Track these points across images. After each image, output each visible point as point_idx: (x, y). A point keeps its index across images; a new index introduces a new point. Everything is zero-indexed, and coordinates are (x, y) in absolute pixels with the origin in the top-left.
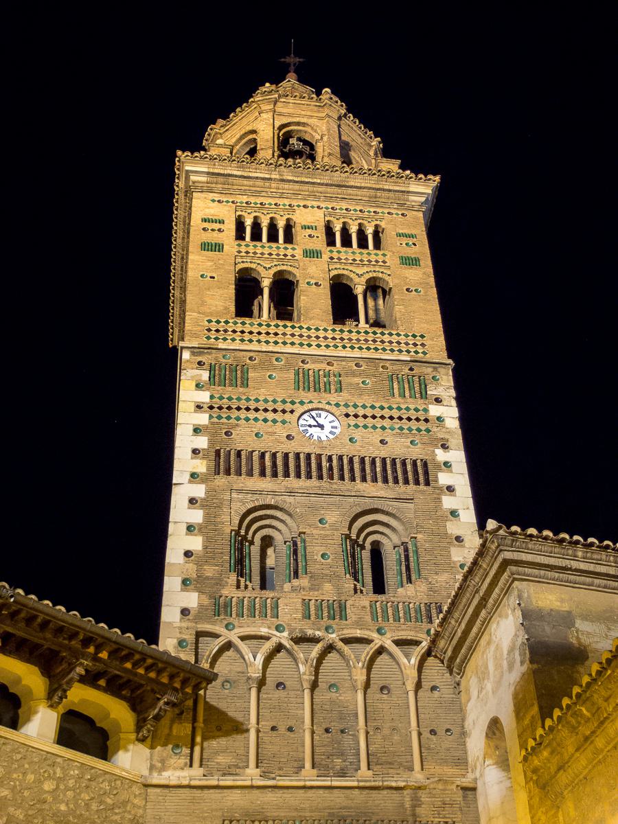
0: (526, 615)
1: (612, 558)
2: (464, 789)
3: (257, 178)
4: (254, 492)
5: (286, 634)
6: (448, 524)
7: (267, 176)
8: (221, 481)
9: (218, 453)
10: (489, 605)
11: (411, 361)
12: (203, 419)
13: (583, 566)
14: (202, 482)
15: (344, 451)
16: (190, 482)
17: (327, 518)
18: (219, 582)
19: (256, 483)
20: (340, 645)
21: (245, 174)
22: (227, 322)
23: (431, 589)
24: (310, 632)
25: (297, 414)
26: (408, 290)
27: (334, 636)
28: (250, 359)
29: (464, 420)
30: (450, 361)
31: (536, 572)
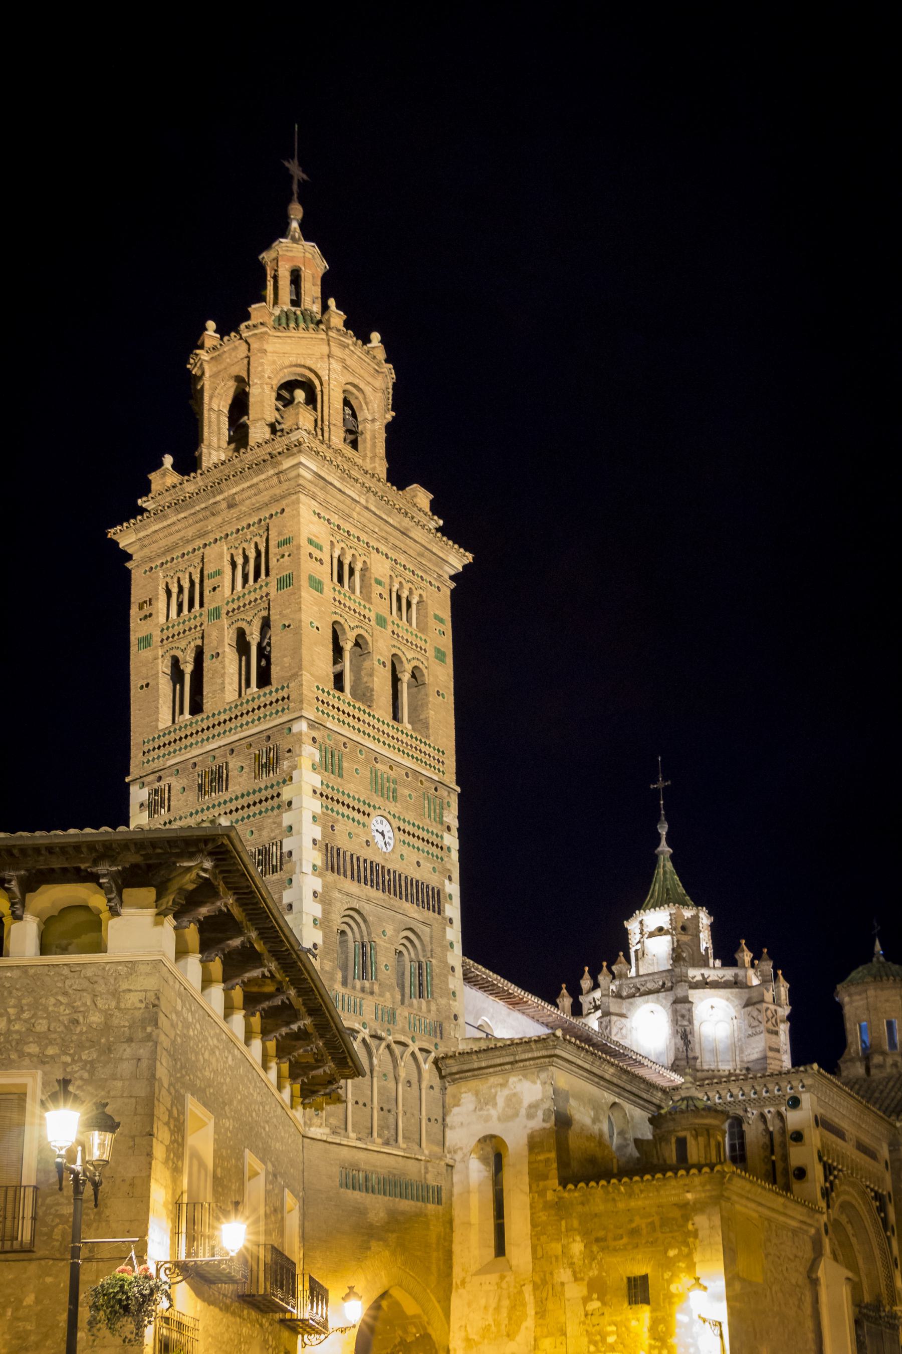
0: (555, 1091)
2: (448, 1165)
4: (347, 894)
5: (367, 1031)
6: (449, 954)
8: (331, 877)
9: (327, 845)
10: (517, 1065)
14: (321, 875)
16: (313, 874)
17: (387, 931)
20: (394, 1046)
23: (438, 1010)
26: (438, 692)
27: (390, 1038)
29: (460, 851)
30: (459, 789)
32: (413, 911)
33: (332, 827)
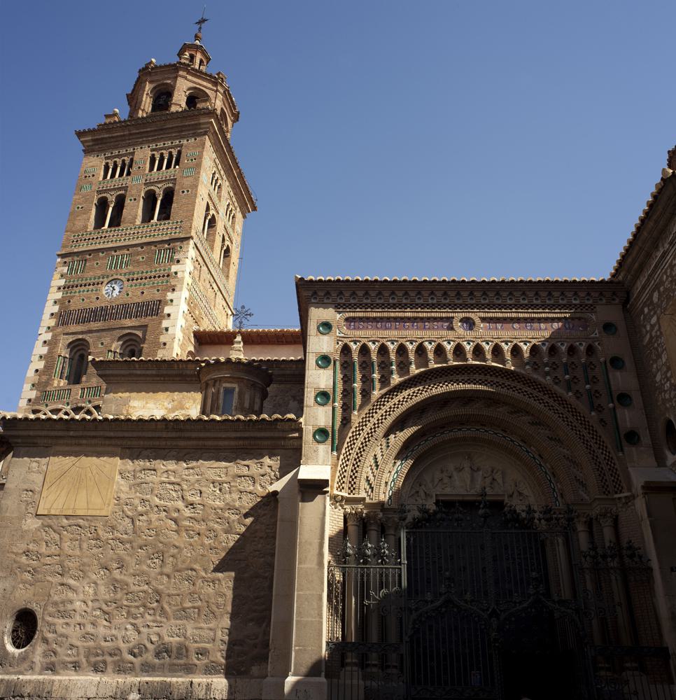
1: (154, 366)
3: (117, 136)
7: (122, 134)
8: (59, 330)
11: (169, 240)
12: (59, 295)
13: (139, 372)
14: (52, 331)
15: (121, 302)
17: (104, 341)
18: (48, 383)
19: (74, 328)
21: (110, 135)
22: (83, 235)
24: (79, 405)
25: (104, 284)
27: (90, 405)
28: (90, 255)
31: (116, 378)
32: (128, 322)
33: (69, 301)
